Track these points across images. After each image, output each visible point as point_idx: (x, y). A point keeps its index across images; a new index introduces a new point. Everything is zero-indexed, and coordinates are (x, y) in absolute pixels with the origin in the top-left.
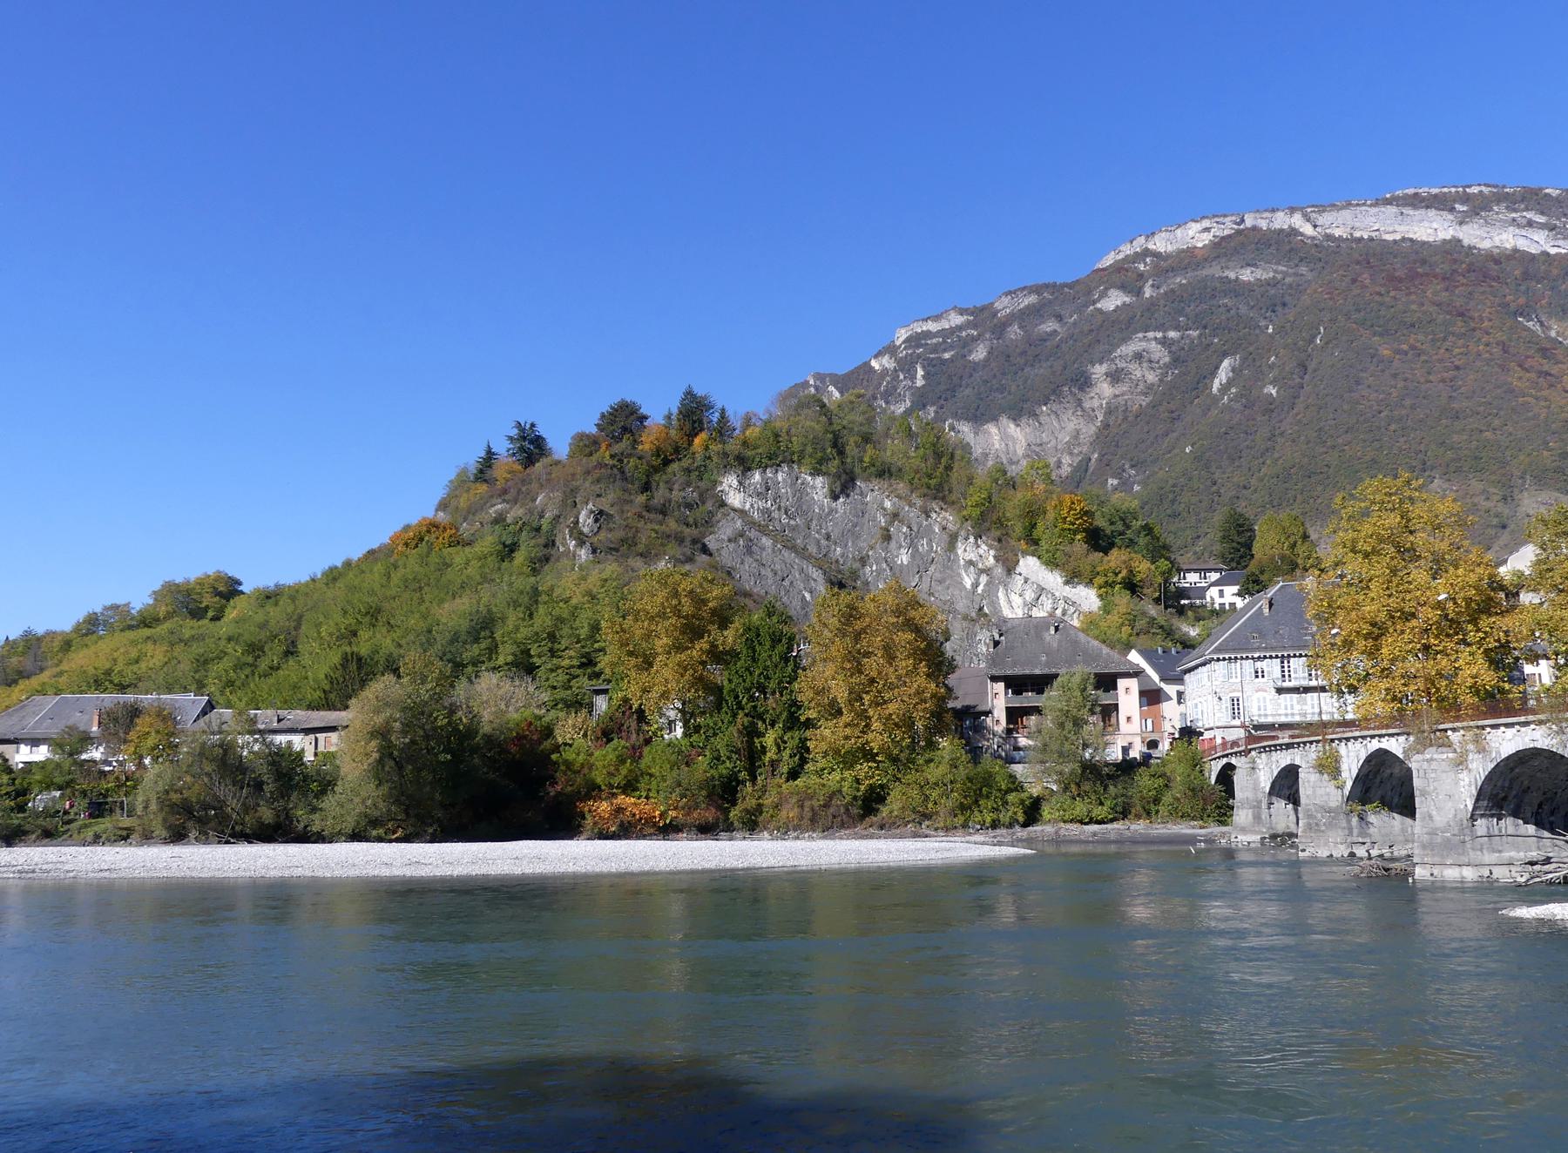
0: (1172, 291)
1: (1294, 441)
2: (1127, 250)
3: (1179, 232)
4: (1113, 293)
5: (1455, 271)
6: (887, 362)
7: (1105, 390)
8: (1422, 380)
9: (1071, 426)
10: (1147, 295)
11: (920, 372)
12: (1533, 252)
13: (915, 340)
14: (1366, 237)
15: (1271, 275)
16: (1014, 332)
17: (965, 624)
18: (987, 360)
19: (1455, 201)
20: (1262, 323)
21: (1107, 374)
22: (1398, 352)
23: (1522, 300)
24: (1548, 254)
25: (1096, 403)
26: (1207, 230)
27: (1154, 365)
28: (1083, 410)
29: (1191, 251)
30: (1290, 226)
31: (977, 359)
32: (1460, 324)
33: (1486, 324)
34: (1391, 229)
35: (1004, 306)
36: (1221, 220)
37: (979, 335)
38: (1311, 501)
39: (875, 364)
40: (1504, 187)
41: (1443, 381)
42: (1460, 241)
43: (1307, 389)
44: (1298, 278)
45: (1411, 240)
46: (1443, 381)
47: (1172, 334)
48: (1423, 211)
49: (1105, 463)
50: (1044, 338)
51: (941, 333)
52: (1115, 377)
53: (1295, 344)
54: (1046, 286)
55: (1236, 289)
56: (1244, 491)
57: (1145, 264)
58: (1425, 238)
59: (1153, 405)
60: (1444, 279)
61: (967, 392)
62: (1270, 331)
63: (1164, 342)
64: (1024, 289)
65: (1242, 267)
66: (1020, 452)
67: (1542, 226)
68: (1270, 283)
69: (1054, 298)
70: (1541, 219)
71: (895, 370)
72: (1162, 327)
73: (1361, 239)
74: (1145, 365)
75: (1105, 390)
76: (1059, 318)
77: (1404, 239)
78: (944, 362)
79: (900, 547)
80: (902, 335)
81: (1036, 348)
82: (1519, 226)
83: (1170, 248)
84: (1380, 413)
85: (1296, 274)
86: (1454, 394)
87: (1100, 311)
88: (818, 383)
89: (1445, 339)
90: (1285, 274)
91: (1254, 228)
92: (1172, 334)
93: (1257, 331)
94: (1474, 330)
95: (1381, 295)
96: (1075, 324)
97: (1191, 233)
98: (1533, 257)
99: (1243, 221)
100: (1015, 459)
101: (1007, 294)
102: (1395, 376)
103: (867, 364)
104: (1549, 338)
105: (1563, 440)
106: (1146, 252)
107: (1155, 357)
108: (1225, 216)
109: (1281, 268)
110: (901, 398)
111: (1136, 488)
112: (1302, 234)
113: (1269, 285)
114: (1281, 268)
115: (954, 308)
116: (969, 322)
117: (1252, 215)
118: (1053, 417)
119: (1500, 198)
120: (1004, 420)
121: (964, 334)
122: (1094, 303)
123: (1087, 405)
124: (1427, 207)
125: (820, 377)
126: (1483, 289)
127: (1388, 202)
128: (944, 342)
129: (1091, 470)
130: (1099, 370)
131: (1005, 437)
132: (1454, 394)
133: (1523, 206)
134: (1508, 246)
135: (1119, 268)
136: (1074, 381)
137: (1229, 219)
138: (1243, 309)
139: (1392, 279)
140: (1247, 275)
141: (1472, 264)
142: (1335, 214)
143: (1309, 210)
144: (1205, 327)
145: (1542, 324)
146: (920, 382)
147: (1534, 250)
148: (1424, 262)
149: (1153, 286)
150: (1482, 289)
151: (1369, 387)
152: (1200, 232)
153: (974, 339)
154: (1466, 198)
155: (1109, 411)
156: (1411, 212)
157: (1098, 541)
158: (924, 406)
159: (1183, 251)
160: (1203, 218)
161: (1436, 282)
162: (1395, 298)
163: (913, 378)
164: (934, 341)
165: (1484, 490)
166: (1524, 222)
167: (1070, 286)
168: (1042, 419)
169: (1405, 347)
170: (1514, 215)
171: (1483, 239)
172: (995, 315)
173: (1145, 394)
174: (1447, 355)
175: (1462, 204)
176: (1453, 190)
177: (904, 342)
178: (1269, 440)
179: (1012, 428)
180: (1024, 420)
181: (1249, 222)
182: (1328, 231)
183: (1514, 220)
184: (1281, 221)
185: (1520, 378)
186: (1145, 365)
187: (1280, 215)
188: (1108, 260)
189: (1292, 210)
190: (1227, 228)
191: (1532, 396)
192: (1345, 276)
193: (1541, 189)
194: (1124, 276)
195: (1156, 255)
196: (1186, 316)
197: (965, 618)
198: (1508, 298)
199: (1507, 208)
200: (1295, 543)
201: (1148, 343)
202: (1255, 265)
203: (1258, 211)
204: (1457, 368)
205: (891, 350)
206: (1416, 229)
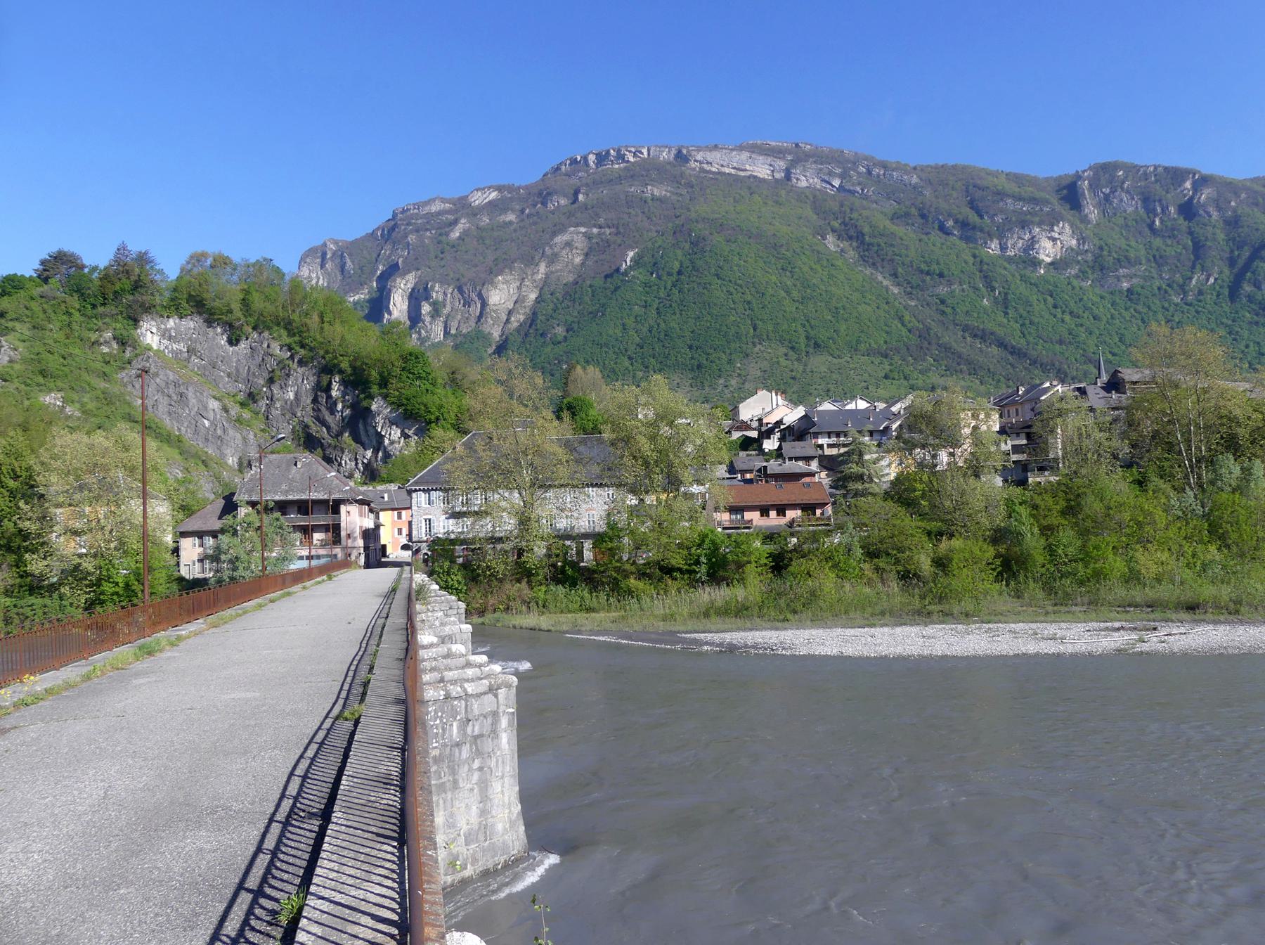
7: (542, 268)
15: (664, 193)
35: (478, 199)
45: (755, 177)
47: (595, 230)
64: (489, 188)
74: (574, 251)
176: (785, 144)
183: (821, 169)
201: (576, 236)
206: (760, 169)
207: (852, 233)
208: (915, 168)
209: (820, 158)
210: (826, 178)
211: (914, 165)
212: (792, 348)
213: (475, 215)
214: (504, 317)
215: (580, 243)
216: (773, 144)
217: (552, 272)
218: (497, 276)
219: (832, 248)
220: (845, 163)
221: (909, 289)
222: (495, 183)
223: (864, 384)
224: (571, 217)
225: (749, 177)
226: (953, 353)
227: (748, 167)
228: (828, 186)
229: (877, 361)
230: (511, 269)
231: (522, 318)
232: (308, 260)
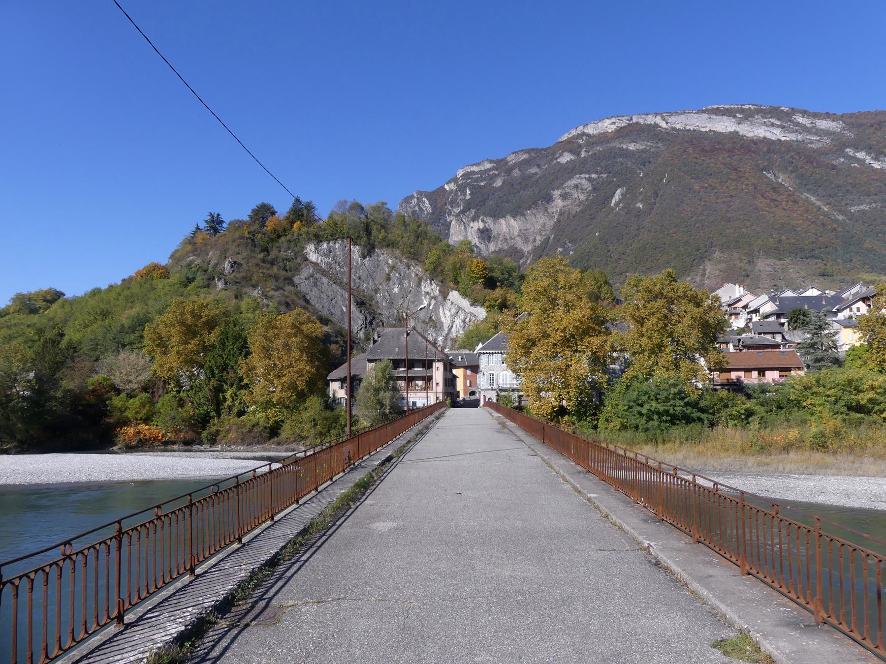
0: (595, 153)
1: (649, 231)
2: (574, 132)
3: (600, 124)
5: (734, 147)
7: (559, 203)
8: (714, 202)
9: (541, 221)
10: (583, 156)
11: (468, 192)
12: (774, 139)
13: (466, 176)
14: (692, 129)
15: (644, 147)
16: (516, 173)
17: (423, 325)
18: (502, 187)
19: (736, 112)
20: (638, 171)
21: (560, 195)
22: (702, 187)
23: (766, 163)
24: (781, 140)
25: (554, 210)
26: (614, 123)
28: (548, 213)
29: (605, 134)
30: (655, 123)
31: (497, 186)
32: (734, 174)
33: (747, 174)
34: (704, 126)
35: (512, 159)
36: (621, 118)
37: (498, 173)
38: (655, 261)
39: (446, 187)
40: (761, 106)
41: (724, 202)
42: (738, 132)
43: (657, 205)
44: (657, 149)
45: (714, 131)
46: (724, 202)
47: (594, 176)
48: (720, 117)
49: (557, 240)
50: (531, 176)
51: (480, 172)
52: (564, 197)
53: (653, 182)
54: (533, 149)
55: (626, 154)
56: (623, 256)
57: (583, 140)
58: (721, 131)
59: (582, 212)
60: (728, 151)
61: (491, 202)
62: (641, 175)
65: (630, 143)
66: (516, 233)
67: (779, 126)
68: (643, 151)
69: (538, 155)
70: (778, 123)
71: (457, 191)
72: (589, 172)
73: (689, 130)
74: (579, 191)
76: (539, 166)
77: (710, 131)
78: (480, 187)
79: (395, 284)
80: (460, 173)
81: (526, 181)
82: (767, 126)
83: (595, 132)
84: (692, 218)
85: (656, 147)
86: (729, 209)
87: (559, 163)
88: (419, 196)
89: (726, 181)
90: (651, 147)
91: (637, 123)
92: (594, 176)
93: (636, 175)
94: (741, 177)
95: (696, 158)
96: (546, 169)
97: (606, 125)
98: (773, 142)
99: (631, 119)
100: (513, 237)
102: (700, 199)
103: (443, 187)
104: (777, 183)
105: (779, 234)
106: (584, 134)
107: (585, 187)
108: (623, 116)
109: (649, 144)
110: (458, 205)
111: (571, 253)
112: (660, 127)
113: (643, 152)
114: (649, 144)
115: (487, 160)
116: (494, 167)
117: (636, 116)
118: (533, 216)
119: (759, 111)
120: (508, 217)
121: (491, 173)
122: (556, 159)
123: (550, 210)
124: (723, 115)
125: (420, 193)
126: (747, 157)
127: (703, 112)
128: (481, 176)
129: (550, 243)
130: (557, 193)
131: (509, 225)
132: (729, 209)
133: (769, 116)
134: (761, 136)
135: (569, 141)
137: (625, 118)
138: (629, 164)
139: (703, 150)
140: (632, 147)
141: (743, 144)
142: (677, 117)
143: (664, 115)
144: (610, 173)
145: (775, 175)
146: (468, 197)
147: (774, 138)
148: (719, 143)
149: (585, 151)
150: (747, 157)
151: (687, 205)
152: (610, 124)
153: (496, 176)
154: (742, 111)
155: (561, 214)
156: (715, 117)
157: (491, 283)
158: (470, 209)
159: (601, 134)
160: (612, 117)
161: (724, 152)
162: (703, 160)
163: (465, 195)
164: (476, 176)
165: (739, 258)
166: (770, 124)
167: (545, 150)
168: (527, 217)
169: (706, 185)
170: (765, 120)
171: (749, 132)
172: (507, 163)
173: (579, 206)
174: (727, 190)
175: (740, 113)
176: (736, 106)
177: (461, 176)
178: (637, 230)
179: (512, 221)
180: (518, 217)
181: (635, 120)
182: (673, 126)
183: (765, 122)
184: (651, 120)
185: (762, 202)
186: (579, 191)
187: (650, 116)
188: (564, 138)
189: (656, 114)
190: (623, 123)
191: (767, 211)
192: (680, 149)
193: (779, 107)
194: (571, 146)
195: (588, 135)
196: (601, 167)
197: (423, 322)
198: (760, 162)
199: (762, 116)
200: (601, 285)
201: (581, 180)
202: (636, 142)
203: (639, 114)
204: (732, 196)
205: (455, 180)
206: (717, 126)
208: (842, 116)
211: (841, 114)
222: (525, 148)
225: (710, 130)
227: (707, 125)
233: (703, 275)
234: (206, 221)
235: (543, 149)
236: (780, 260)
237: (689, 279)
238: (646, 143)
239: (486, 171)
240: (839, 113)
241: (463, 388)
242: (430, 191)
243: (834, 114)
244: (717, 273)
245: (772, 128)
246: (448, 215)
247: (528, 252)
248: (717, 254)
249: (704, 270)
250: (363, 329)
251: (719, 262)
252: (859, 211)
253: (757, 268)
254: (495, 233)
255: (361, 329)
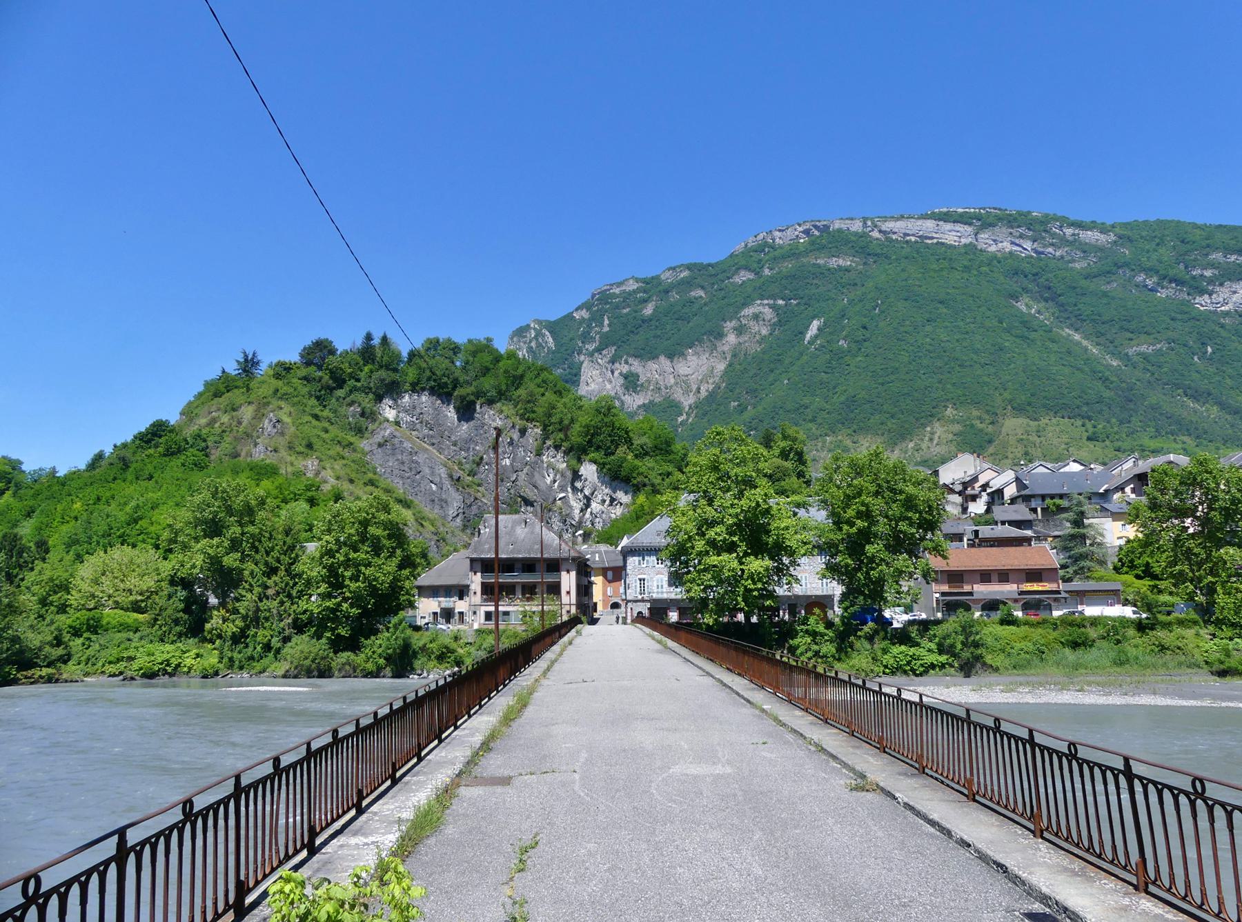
4: (742, 273)
6: (584, 314)
7: (732, 338)
11: (606, 322)
15: (849, 263)
16: (675, 296)
27: (766, 323)
35: (668, 277)
45: (943, 244)
47: (781, 302)
52: (740, 330)
55: (824, 273)
59: (764, 352)
63: (773, 307)
64: (679, 267)
68: (847, 270)
70: (1030, 233)
72: (774, 297)
74: (761, 323)
75: (732, 338)
97: (797, 233)
100: (669, 385)
101: (669, 269)
104: (1030, 314)
110: (593, 340)
120: (662, 358)
136: (710, 333)
140: (834, 262)
143: (876, 220)
146: (606, 329)
163: (602, 325)
166: (1018, 234)
173: (760, 343)
176: (972, 210)
183: (1011, 233)
186: (761, 323)
193: (1029, 212)
202: (838, 257)
207: (1048, 294)
208: (1113, 226)
209: (1011, 221)
210: (1017, 241)
212: (988, 412)
213: (668, 292)
214: (694, 387)
215: (768, 313)
216: (960, 210)
217: (740, 343)
218: (687, 349)
219: (1024, 308)
220: (1037, 227)
221: (1111, 348)
222: (686, 262)
223: (1063, 446)
224: (761, 291)
226: (1161, 414)
227: (935, 235)
228: (1020, 249)
229: (1079, 423)
230: (700, 341)
231: (711, 387)
232: (515, 339)
233: (931, 440)
234: (238, 361)
235: (709, 265)
236: (1036, 420)
237: (911, 445)
238: (851, 258)
239: (630, 294)
240: (1109, 222)
241: (601, 598)
242: (552, 320)
243: (1103, 224)
244: (951, 436)
245: (1021, 241)
246: (578, 354)
247: (690, 407)
248: (950, 411)
249: (933, 433)
250: (461, 515)
251: (953, 422)
252: (1138, 354)
253: (1004, 430)
254: (642, 379)
255: (458, 515)
